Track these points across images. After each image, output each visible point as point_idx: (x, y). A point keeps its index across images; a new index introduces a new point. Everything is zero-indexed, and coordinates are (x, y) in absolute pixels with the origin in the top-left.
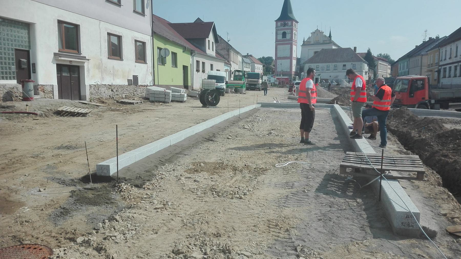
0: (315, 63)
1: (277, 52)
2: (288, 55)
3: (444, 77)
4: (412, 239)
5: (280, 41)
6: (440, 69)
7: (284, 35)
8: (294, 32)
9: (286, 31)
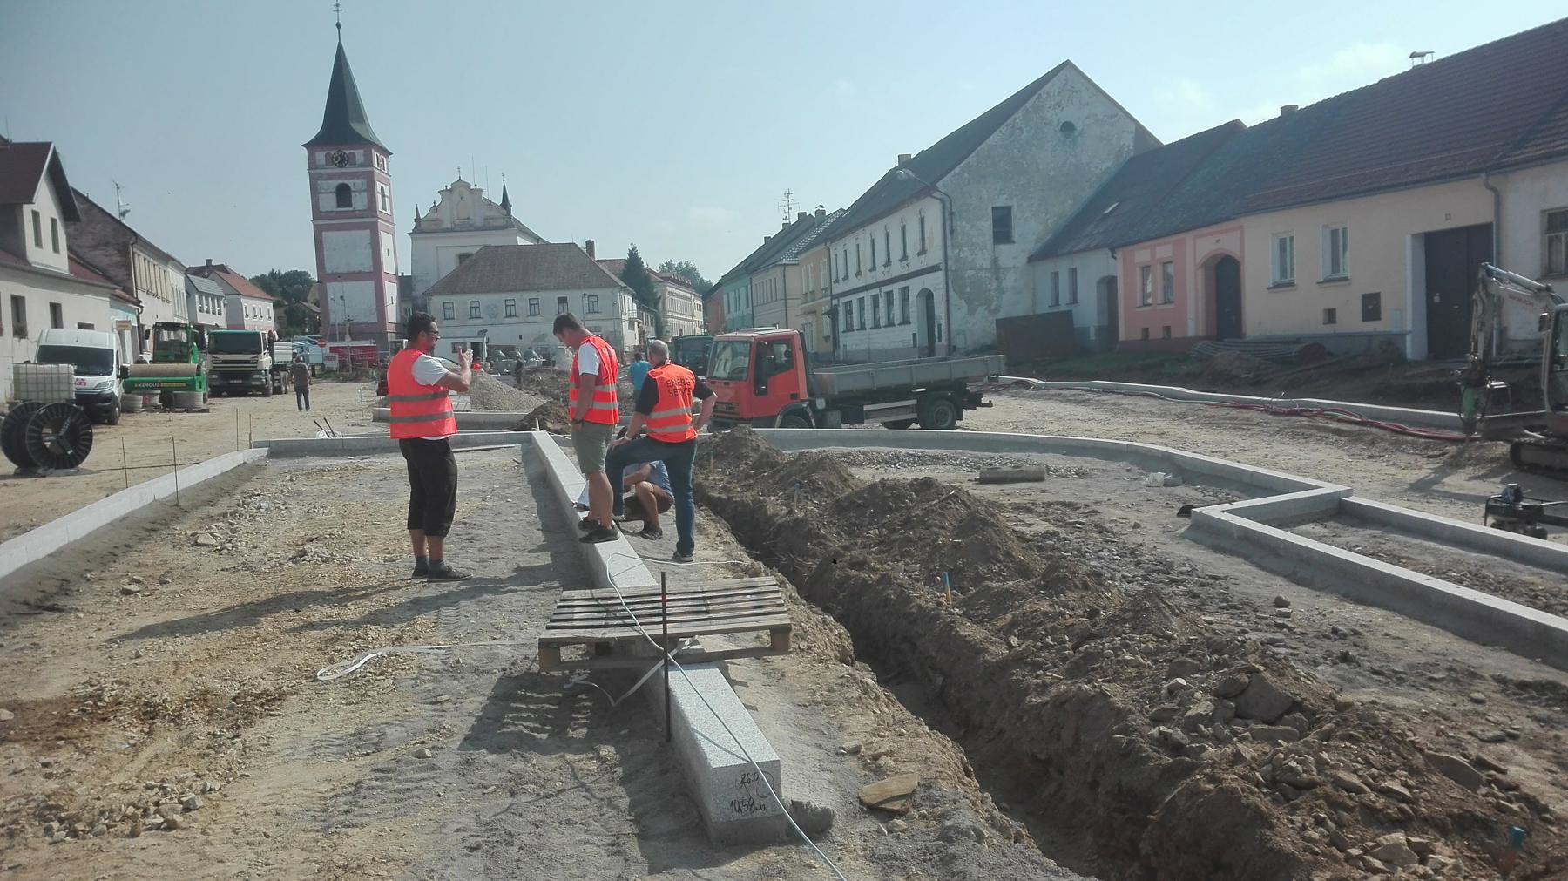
0: (463, 292)
2: (367, 266)
3: (849, 329)
4: (766, 851)
5: (328, 215)
6: (837, 306)
7: (343, 194)
8: (378, 186)
9: (350, 182)
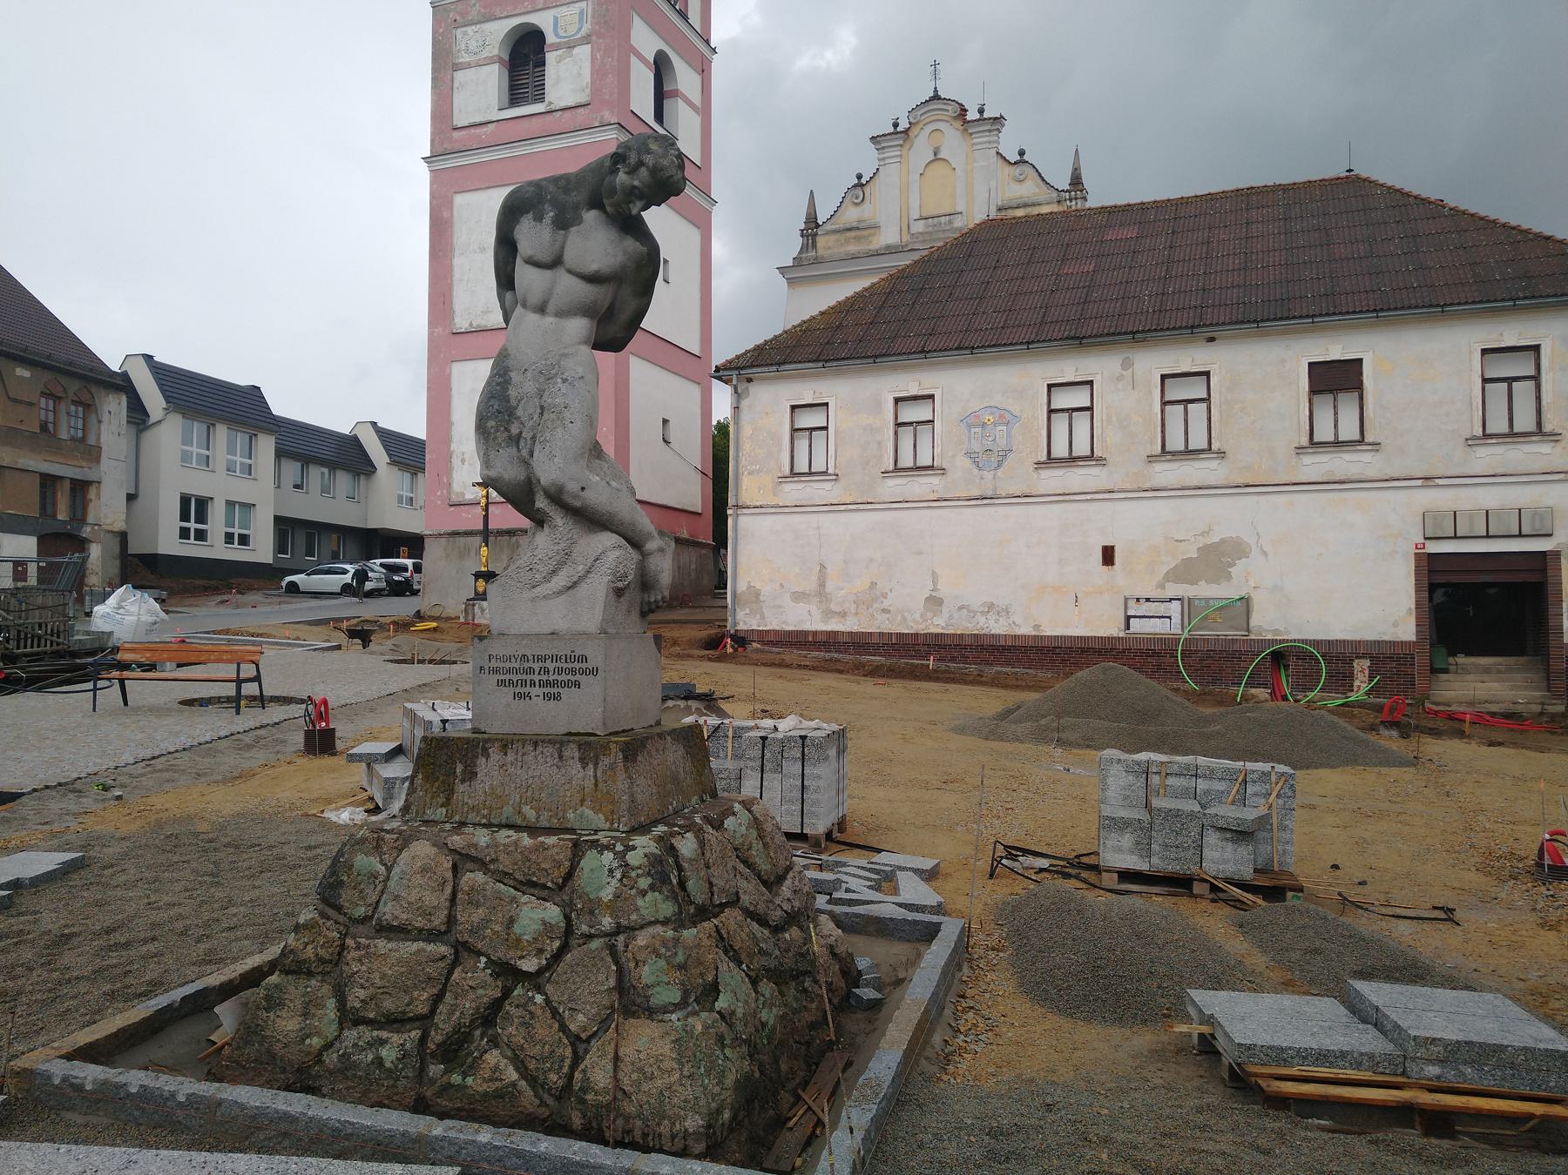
1: (450, 268)
9: (543, 20)
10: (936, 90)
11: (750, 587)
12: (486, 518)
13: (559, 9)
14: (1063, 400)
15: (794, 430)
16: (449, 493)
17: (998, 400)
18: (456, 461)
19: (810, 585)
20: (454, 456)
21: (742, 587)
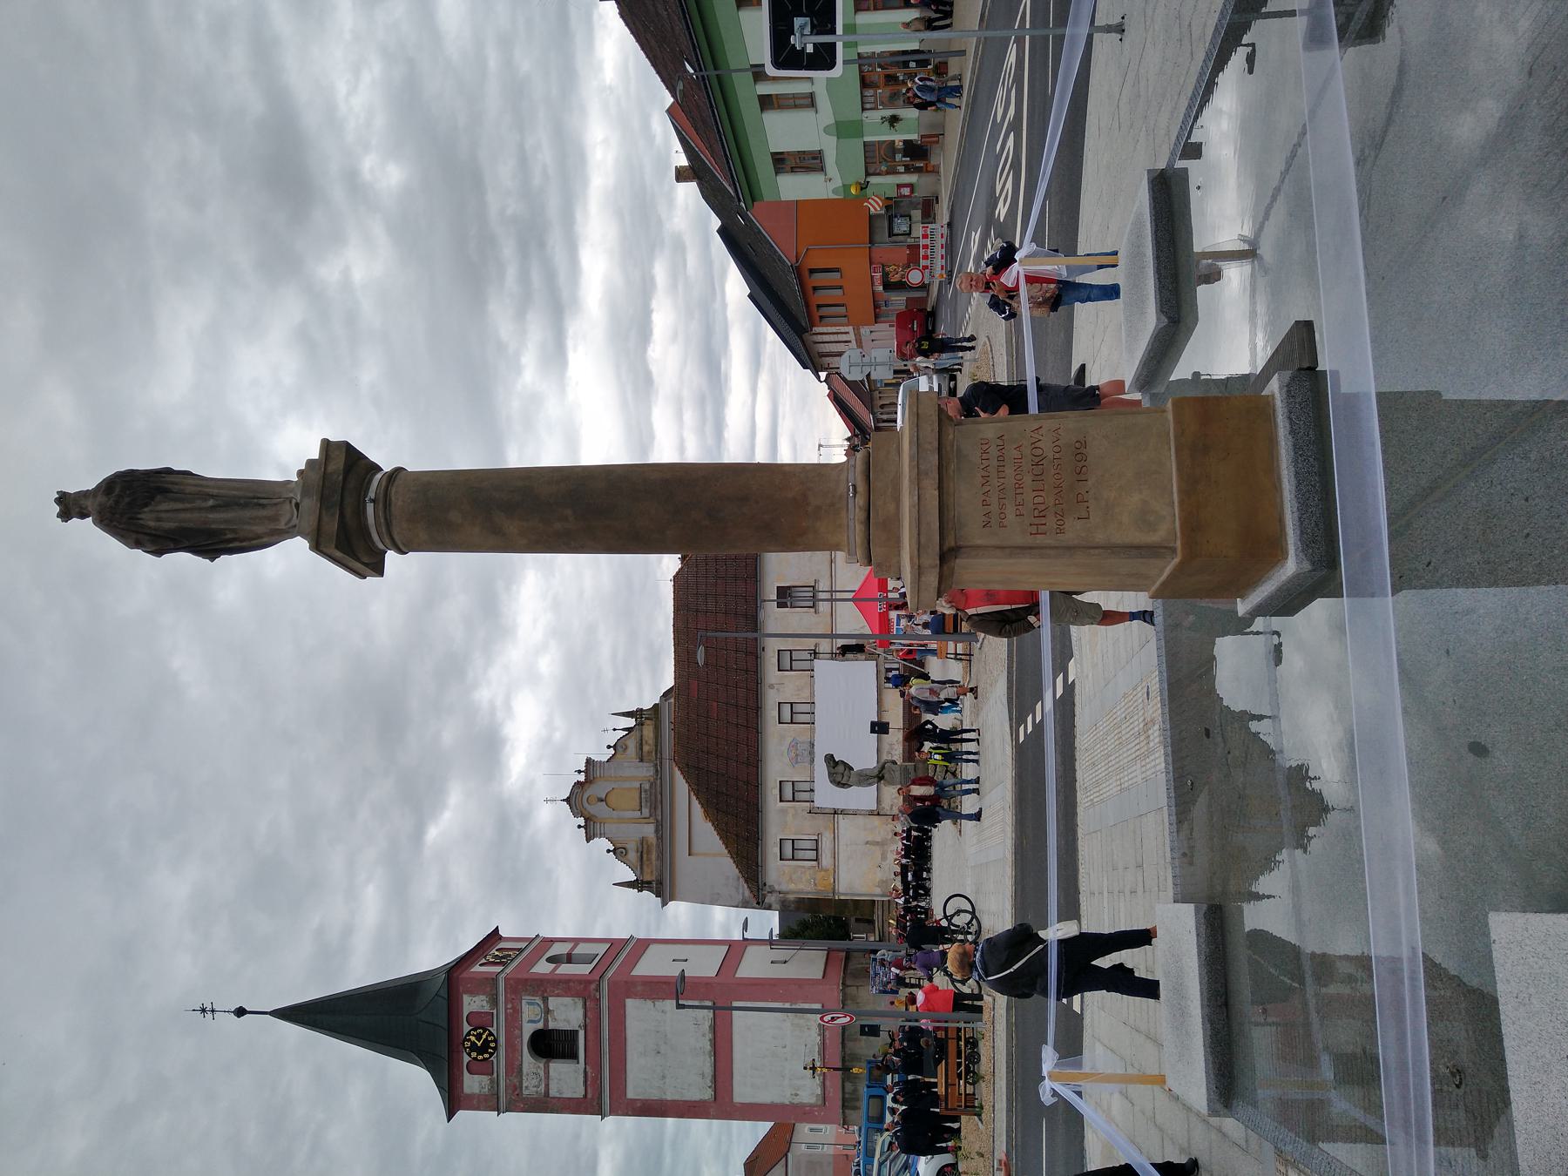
5: (592, 1081)
7: (550, 1045)
8: (543, 968)
9: (528, 1030)
10: (564, 800)
11: (878, 886)
12: (835, 1069)
13: (524, 1019)
14: (787, 716)
15: (793, 859)
16: (817, 1106)
17: (785, 748)
18: (795, 1101)
19: (877, 851)
20: (793, 1101)
21: (878, 891)
